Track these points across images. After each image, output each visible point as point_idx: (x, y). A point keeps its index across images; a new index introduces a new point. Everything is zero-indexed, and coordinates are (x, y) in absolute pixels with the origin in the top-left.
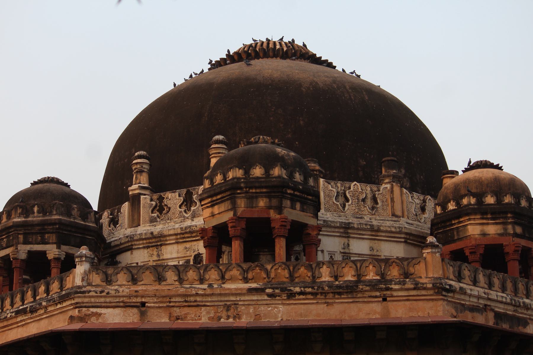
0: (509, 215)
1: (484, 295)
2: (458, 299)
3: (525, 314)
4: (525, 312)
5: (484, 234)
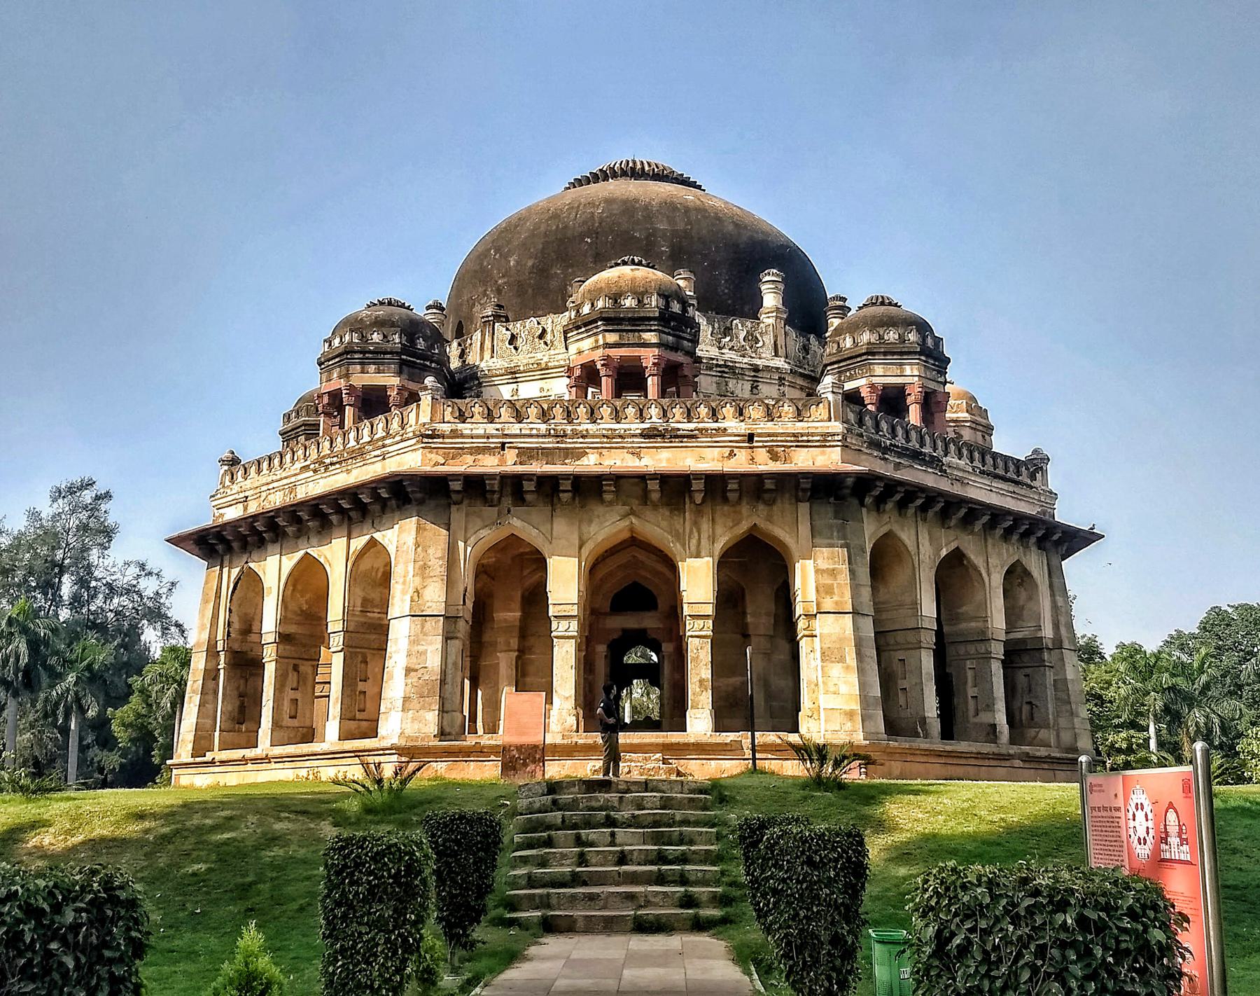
1: (497, 432)
2: (452, 443)
3: (581, 443)
4: (581, 440)
5: (580, 353)
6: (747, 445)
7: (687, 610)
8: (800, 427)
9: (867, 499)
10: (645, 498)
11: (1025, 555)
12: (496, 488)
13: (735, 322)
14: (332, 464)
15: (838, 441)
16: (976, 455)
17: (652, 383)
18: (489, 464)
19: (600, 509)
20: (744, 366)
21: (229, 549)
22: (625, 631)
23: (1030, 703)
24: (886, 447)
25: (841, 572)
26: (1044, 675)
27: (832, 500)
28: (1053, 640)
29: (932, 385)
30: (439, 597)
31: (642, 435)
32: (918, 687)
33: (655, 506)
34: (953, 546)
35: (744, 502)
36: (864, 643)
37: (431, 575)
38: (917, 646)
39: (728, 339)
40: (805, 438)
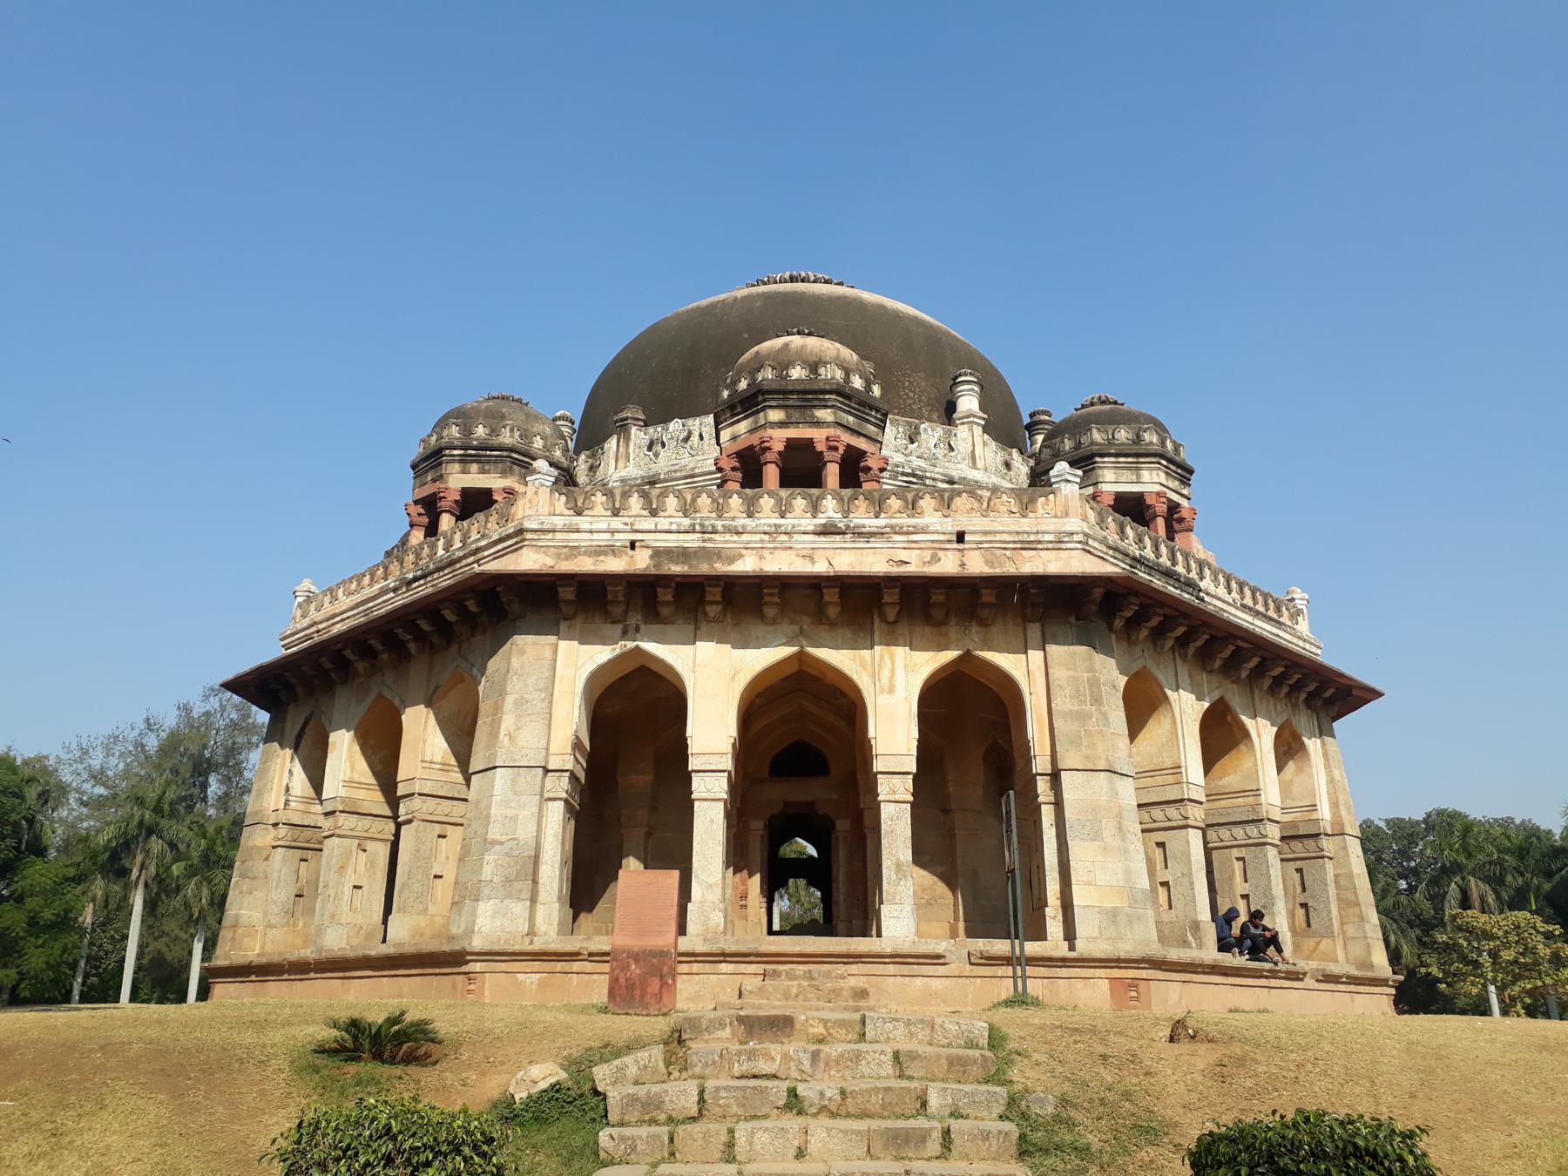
0: (760, 398)
2: (563, 540)
3: (735, 542)
4: (736, 538)
6: (956, 546)
7: (878, 765)
8: (1025, 524)
9: (1117, 621)
10: (820, 617)
11: (1294, 715)
12: (621, 597)
13: (923, 426)
14: (416, 579)
15: (1080, 542)
16: (1234, 585)
17: (832, 472)
18: (614, 565)
19: (758, 630)
20: (936, 476)
21: (294, 698)
22: (787, 804)
23: (1304, 906)
24: (1134, 559)
25: (1090, 716)
26: (1323, 868)
27: (1072, 619)
28: (1332, 823)
29: (1175, 497)
30: (539, 741)
31: (814, 533)
32: (1185, 880)
33: (833, 625)
34: (1216, 696)
35: (953, 622)
36: (1125, 814)
37: (530, 712)
38: (1181, 823)
39: (916, 444)
40: (1032, 538)
